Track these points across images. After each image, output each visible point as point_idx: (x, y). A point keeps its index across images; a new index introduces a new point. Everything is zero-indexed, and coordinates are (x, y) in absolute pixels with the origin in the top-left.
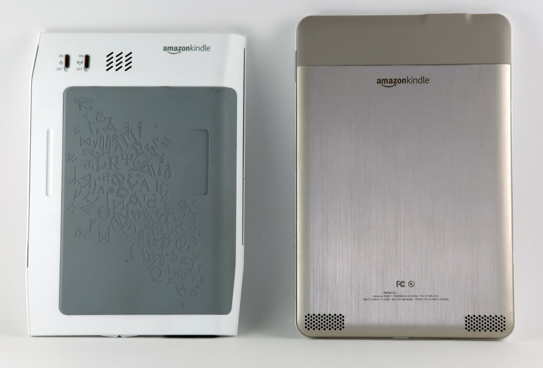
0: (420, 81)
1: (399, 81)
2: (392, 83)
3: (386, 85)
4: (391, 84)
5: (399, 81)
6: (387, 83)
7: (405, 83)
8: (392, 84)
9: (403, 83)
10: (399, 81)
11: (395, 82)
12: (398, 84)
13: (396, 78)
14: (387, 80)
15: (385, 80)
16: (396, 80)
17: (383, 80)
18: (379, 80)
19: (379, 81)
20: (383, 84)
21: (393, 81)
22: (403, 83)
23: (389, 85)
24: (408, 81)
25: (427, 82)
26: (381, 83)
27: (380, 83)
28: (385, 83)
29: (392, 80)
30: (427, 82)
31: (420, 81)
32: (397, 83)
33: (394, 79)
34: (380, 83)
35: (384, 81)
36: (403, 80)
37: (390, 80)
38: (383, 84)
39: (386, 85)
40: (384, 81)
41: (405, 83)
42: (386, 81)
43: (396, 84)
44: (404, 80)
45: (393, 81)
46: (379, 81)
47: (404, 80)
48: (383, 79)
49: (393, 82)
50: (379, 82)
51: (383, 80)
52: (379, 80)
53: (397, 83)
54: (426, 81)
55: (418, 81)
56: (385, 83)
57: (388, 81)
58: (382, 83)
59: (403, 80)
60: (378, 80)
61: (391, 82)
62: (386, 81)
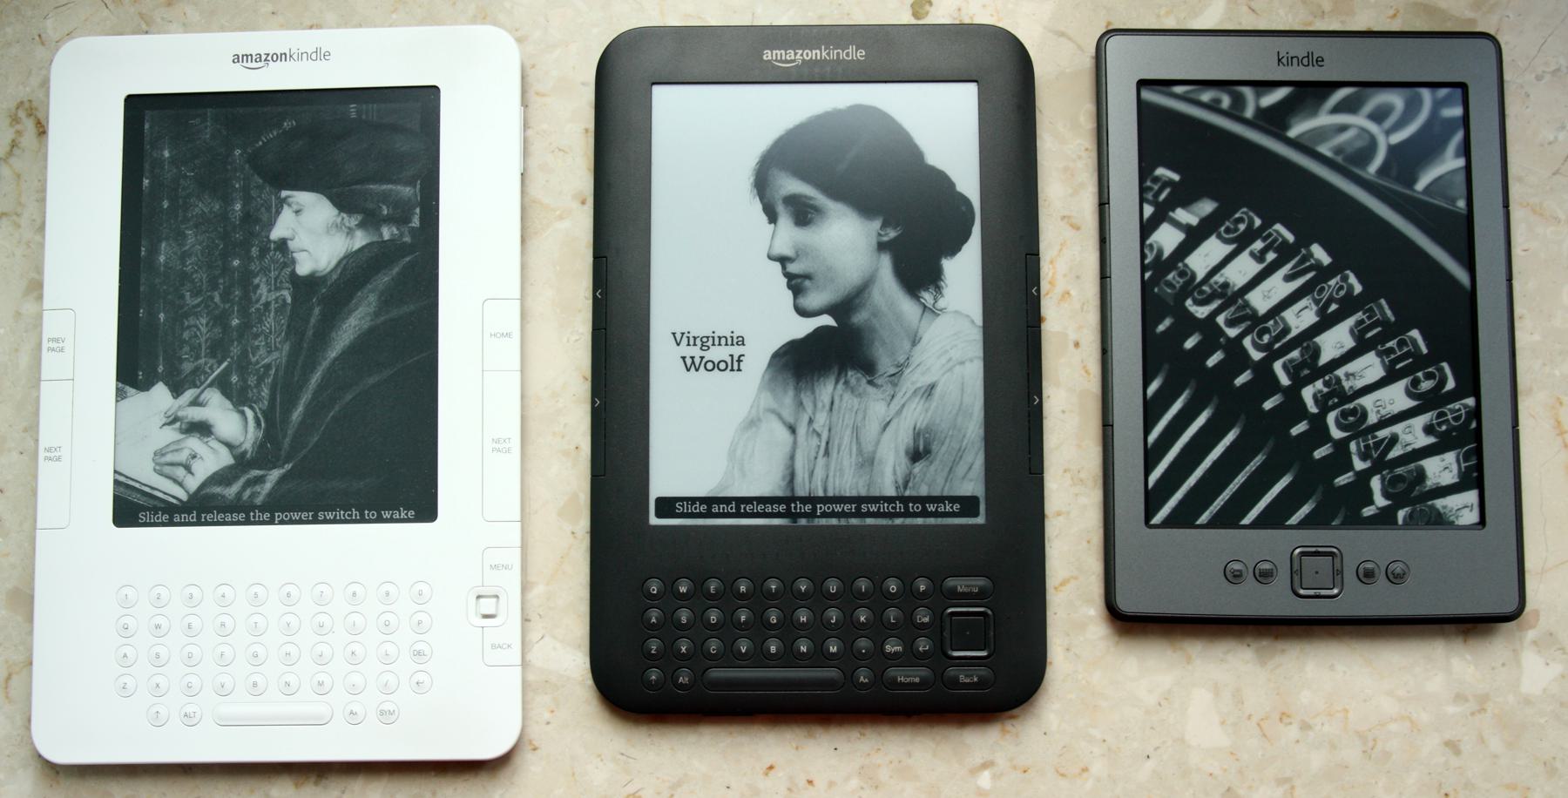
0: (314, 56)
1: (275, 59)
2: (260, 61)
3: (250, 65)
5: (275, 57)
7: (286, 60)
8: (260, 64)
9: (281, 60)
10: (275, 57)
11: (266, 60)
12: (271, 63)
14: (251, 55)
15: (247, 56)
16: (268, 55)
19: (237, 59)
21: (264, 57)
23: (254, 65)
24: (291, 56)
25: (326, 57)
27: (238, 61)
28: (247, 61)
30: (326, 57)
31: (314, 56)
34: (238, 61)
35: (245, 57)
36: (281, 54)
40: (245, 57)
41: (286, 60)
42: (250, 57)
44: (283, 56)
45: (264, 57)
46: (237, 59)
47: (283, 56)
49: (263, 59)
51: (243, 56)
54: (326, 56)
55: (309, 57)
56: (247, 61)
59: (281, 54)
62: (250, 57)
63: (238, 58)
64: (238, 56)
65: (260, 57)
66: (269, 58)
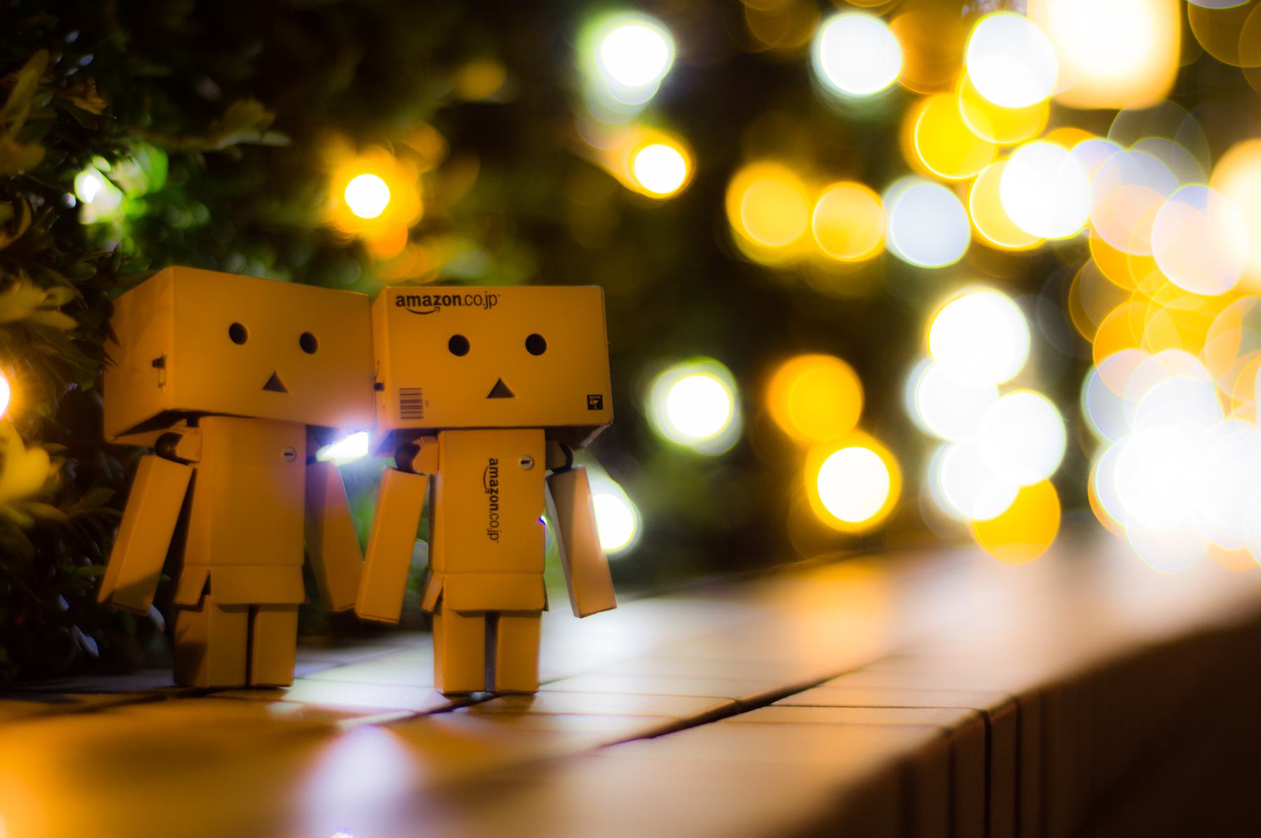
2: (430, 304)
3: (417, 308)
4: (429, 307)
5: (447, 300)
6: (419, 305)
7: (460, 304)
9: (454, 304)
10: (447, 300)
11: (436, 303)
12: (442, 307)
13: (438, 294)
14: (418, 297)
15: (413, 298)
16: (438, 297)
17: (408, 298)
18: (400, 299)
20: (412, 308)
21: (433, 300)
22: (454, 304)
23: (423, 309)
26: (406, 306)
28: (414, 305)
29: (429, 297)
32: (440, 304)
33: (435, 297)
34: (404, 305)
35: (411, 300)
36: (454, 297)
37: (424, 297)
38: (412, 308)
39: (417, 308)
40: (411, 300)
41: (460, 304)
42: (417, 300)
43: (439, 308)
44: (457, 300)
45: (433, 300)
47: (457, 300)
48: (410, 295)
50: (400, 303)
52: (400, 299)
53: (440, 304)
57: (422, 300)
58: (409, 305)
60: (398, 297)
61: (427, 303)
62: (417, 300)
63: (403, 301)
64: (403, 298)
65: (429, 300)
66: (440, 301)
